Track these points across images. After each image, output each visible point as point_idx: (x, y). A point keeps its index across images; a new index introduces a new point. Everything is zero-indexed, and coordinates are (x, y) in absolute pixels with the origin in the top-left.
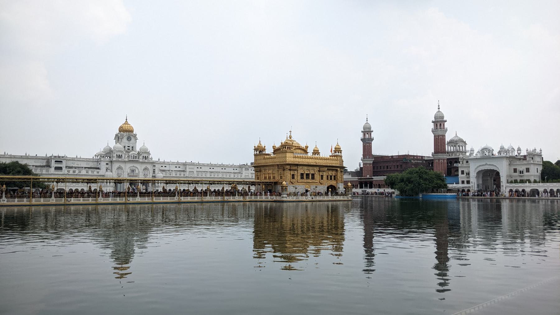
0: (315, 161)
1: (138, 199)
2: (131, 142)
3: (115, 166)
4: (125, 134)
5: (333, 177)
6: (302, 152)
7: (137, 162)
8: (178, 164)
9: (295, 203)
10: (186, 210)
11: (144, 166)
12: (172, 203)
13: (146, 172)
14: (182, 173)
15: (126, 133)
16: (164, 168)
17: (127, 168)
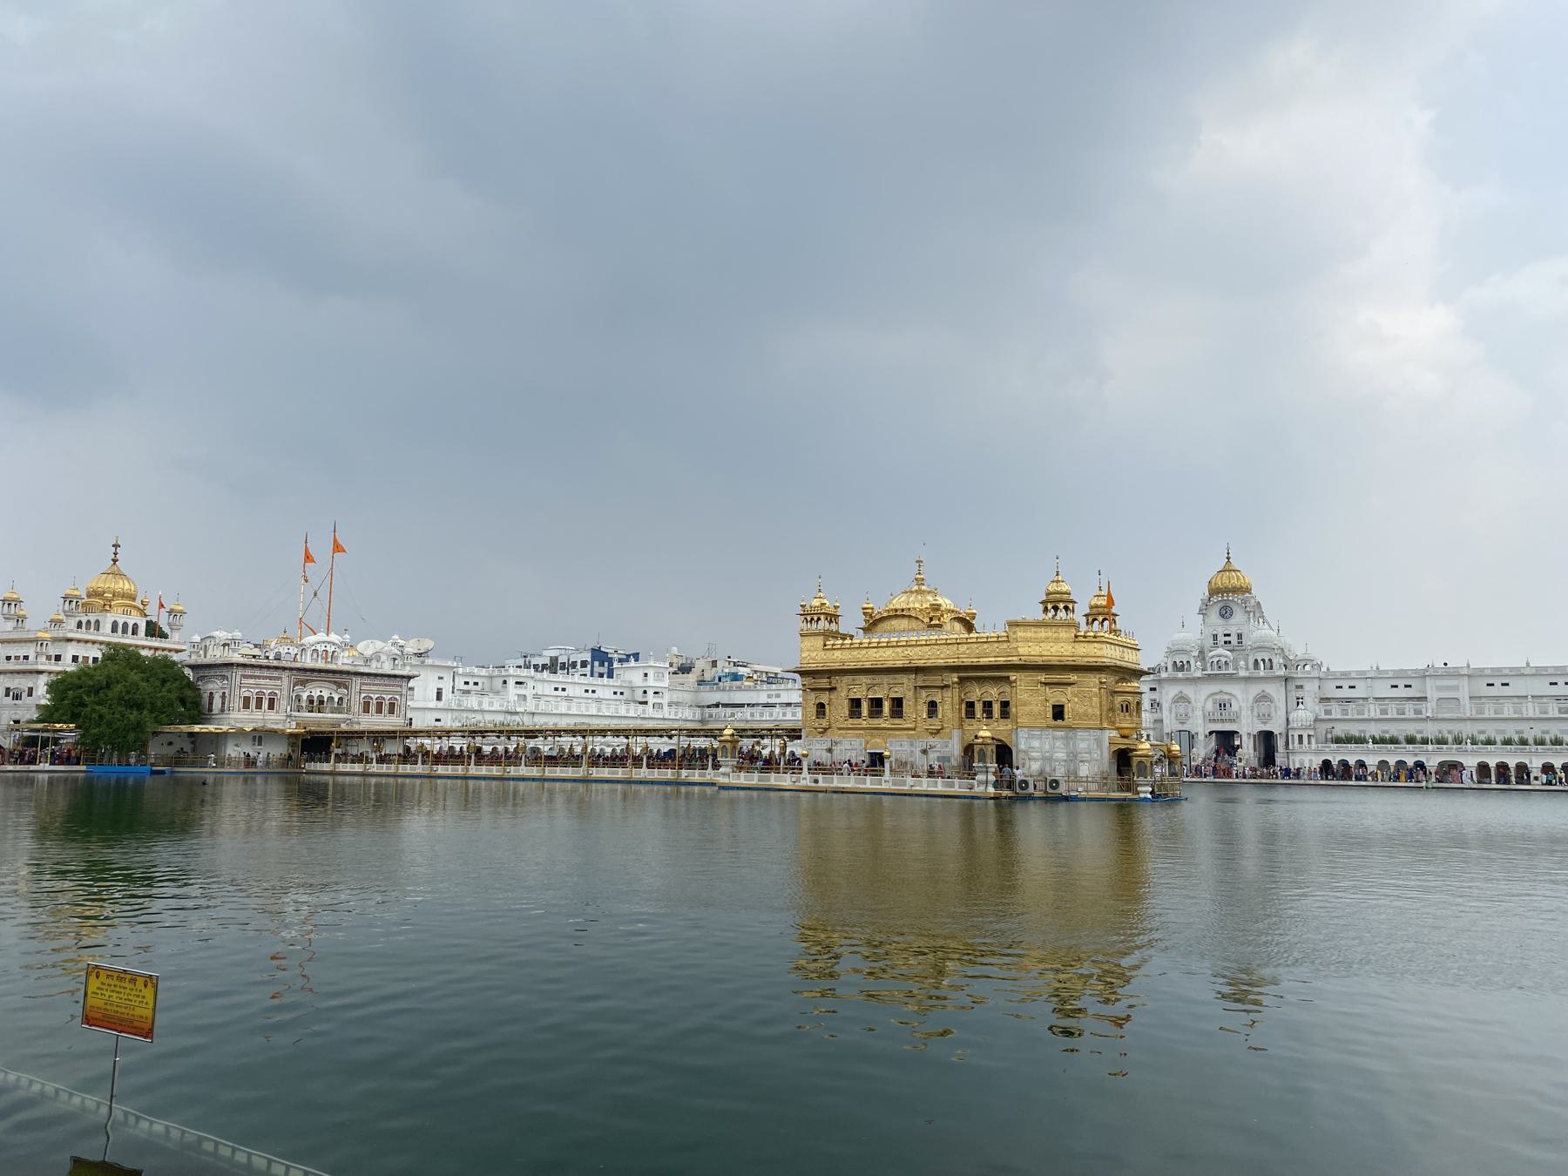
0: (909, 651)
1: (523, 770)
2: (1232, 621)
3: (1168, 694)
4: (1214, 599)
5: (996, 708)
6: (914, 624)
7: (1230, 678)
8: (1400, 678)
9: (755, 794)
10: (732, 802)
11: (1255, 690)
12: (575, 781)
13: (1264, 708)
14: (1409, 709)
15: (1227, 596)
16: (1346, 693)
17: (1202, 698)
